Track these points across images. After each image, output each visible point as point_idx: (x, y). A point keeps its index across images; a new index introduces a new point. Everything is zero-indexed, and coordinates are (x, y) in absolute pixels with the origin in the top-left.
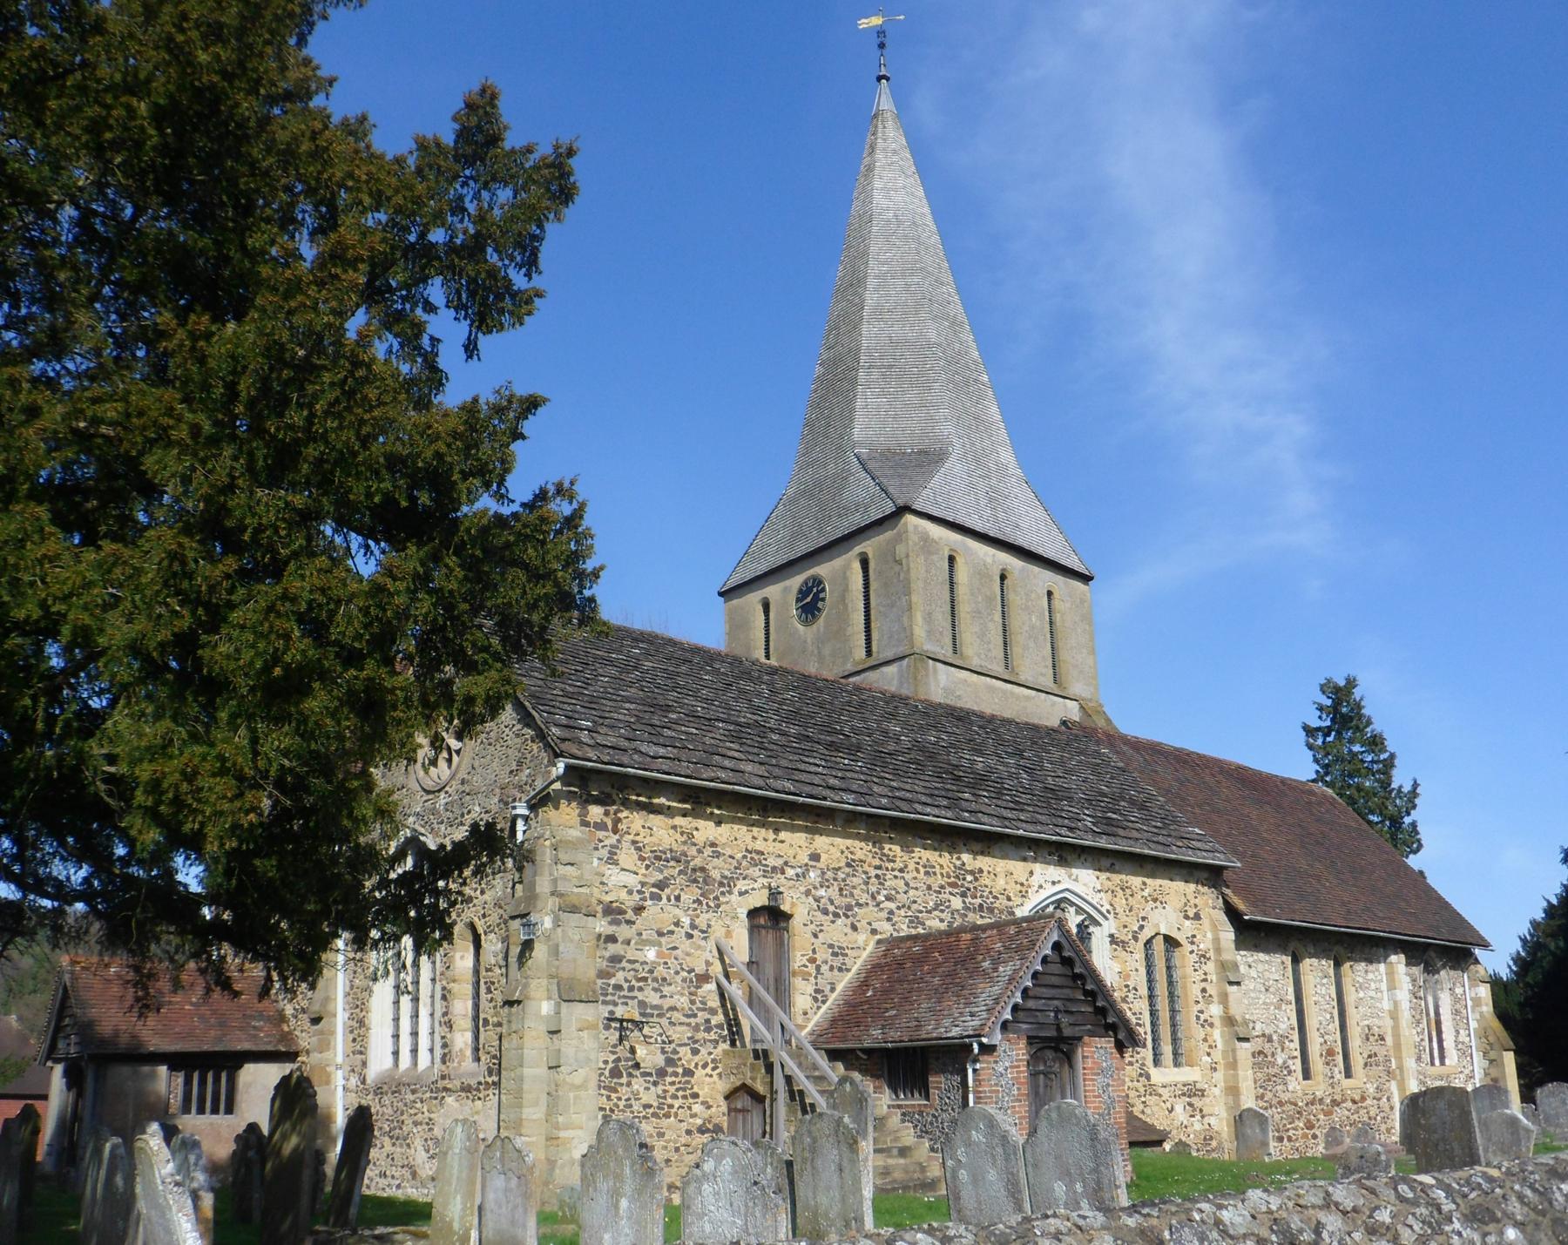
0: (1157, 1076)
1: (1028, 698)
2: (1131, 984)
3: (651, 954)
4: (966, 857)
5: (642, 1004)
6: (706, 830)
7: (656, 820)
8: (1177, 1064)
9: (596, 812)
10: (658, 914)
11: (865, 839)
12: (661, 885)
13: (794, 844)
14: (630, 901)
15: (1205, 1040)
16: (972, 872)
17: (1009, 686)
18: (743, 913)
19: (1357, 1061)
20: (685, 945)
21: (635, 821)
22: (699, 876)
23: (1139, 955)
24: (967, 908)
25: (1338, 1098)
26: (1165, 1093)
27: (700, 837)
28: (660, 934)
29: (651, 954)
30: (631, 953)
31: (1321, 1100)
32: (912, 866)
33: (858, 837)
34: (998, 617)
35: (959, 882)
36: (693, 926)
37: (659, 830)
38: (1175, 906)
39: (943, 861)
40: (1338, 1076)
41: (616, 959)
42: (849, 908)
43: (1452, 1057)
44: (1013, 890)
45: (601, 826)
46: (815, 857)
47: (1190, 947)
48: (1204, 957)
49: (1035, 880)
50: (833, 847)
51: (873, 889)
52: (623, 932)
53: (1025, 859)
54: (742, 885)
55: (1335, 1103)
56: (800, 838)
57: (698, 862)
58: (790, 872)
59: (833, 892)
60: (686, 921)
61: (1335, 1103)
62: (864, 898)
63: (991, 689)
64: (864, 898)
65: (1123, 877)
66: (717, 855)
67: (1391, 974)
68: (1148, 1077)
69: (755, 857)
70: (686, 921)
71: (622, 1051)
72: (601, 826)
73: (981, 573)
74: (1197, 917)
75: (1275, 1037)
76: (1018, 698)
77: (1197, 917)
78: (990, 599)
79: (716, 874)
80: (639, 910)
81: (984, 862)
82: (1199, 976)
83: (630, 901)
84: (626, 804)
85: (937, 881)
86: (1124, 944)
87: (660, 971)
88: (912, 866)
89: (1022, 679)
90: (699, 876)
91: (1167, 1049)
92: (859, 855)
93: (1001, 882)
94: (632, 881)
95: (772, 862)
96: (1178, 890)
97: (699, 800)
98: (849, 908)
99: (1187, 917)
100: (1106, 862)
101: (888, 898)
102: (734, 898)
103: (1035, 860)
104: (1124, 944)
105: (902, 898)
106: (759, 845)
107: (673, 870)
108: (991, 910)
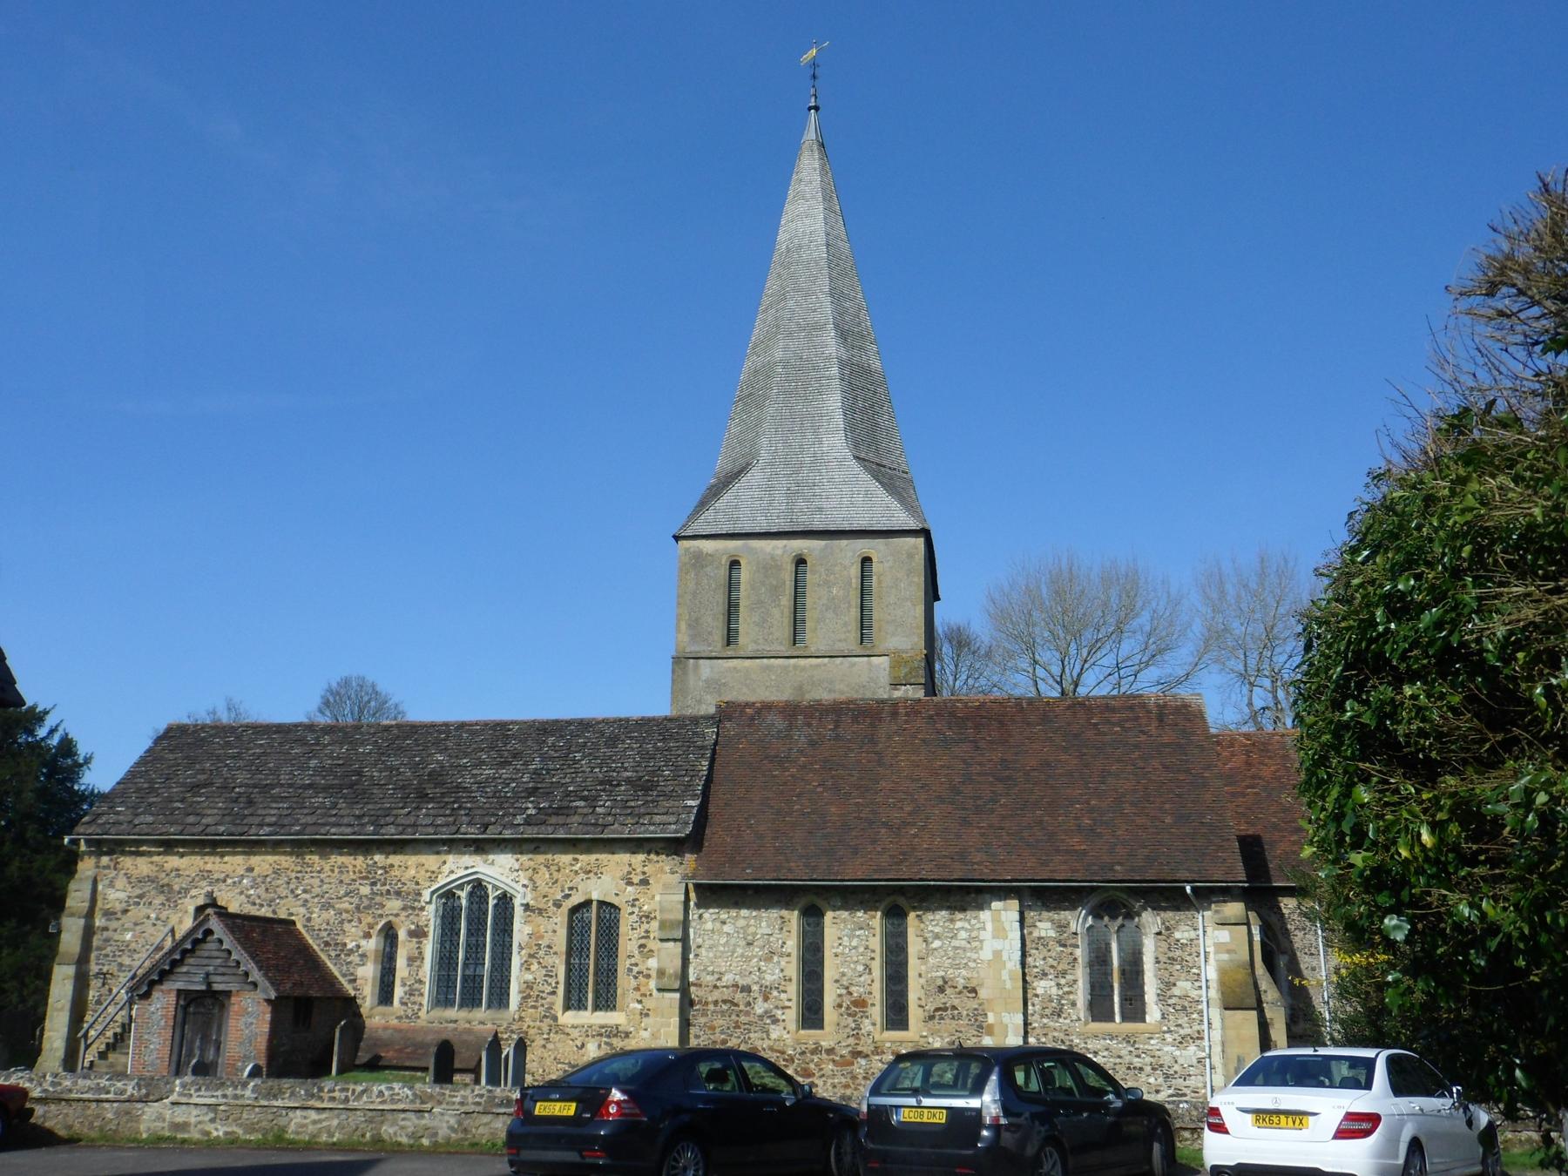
0: (569, 1018)
1: (818, 666)
2: (544, 943)
3: (128, 936)
4: (377, 858)
5: (121, 965)
6: (173, 861)
7: (141, 861)
8: (596, 1008)
9: (105, 860)
10: (137, 913)
11: (291, 854)
12: (141, 896)
13: (235, 863)
14: (119, 907)
15: (637, 989)
16: (383, 868)
17: (802, 662)
18: (191, 909)
19: (915, 1014)
20: (151, 930)
21: (127, 862)
22: (166, 889)
23: (560, 920)
24: (373, 893)
25: (866, 1049)
26: (575, 1033)
27: (168, 867)
28: (136, 924)
29: (128, 936)
30: (116, 937)
31: (830, 1051)
32: (327, 868)
33: (285, 853)
34: (786, 601)
35: (369, 876)
36: (158, 919)
37: (142, 866)
38: (604, 878)
39: (360, 861)
40: (866, 1026)
41: (107, 940)
42: (273, 900)
43: (1153, 1013)
44: (422, 876)
45: (108, 867)
46: (251, 870)
47: (630, 910)
48: (648, 917)
49: (446, 869)
50: (263, 863)
51: (292, 886)
52: (113, 924)
53: (438, 853)
54: (193, 892)
55: (857, 1054)
56: (239, 859)
57: (166, 881)
58: (229, 881)
59: (261, 891)
60: (153, 916)
61: (857, 1054)
62: (283, 891)
63: (768, 668)
64: (283, 891)
65: (549, 856)
66: (179, 876)
67: (996, 920)
68: (555, 1019)
69: (205, 875)
70: (153, 916)
71: (105, 990)
72: (108, 867)
73: (768, 567)
74: (645, 882)
75: (755, 988)
76: (803, 669)
77: (645, 882)
78: (775, 590)
79: (176, 888)
80: (125, 911)
81: (395, 859)
82: (635, 935)
83: (119, 907)
84: (123, 853)
85: (346, 878)
86: (540, 911)
87: (133, 946)
88: (327, 868)
89: (813, 650)
90: (166, 889)
91: (575, 997)
92: (285, 865)
93: (412, 872)
94: (122, 895)
95: (216, 876)
96: (620, 861)
97: (169, 846)
98: (273, 900)
99: (630, 883)
100: (525, 847)
101: (305, 891)
102: (187, 900)
103: (449, 852)
104: (540, 911)
105: (317, 890)
106: (209, 867)
107: (149, 887)
108: (398, 893)
